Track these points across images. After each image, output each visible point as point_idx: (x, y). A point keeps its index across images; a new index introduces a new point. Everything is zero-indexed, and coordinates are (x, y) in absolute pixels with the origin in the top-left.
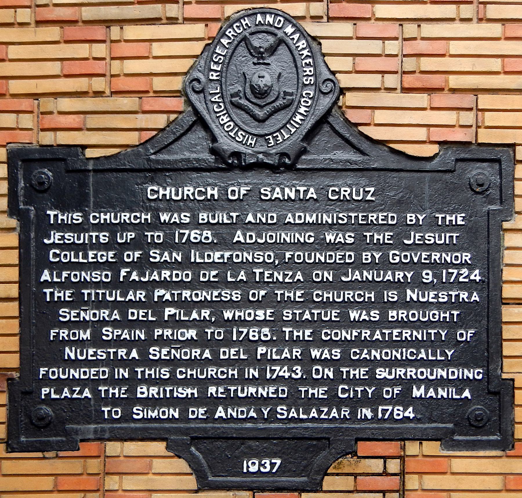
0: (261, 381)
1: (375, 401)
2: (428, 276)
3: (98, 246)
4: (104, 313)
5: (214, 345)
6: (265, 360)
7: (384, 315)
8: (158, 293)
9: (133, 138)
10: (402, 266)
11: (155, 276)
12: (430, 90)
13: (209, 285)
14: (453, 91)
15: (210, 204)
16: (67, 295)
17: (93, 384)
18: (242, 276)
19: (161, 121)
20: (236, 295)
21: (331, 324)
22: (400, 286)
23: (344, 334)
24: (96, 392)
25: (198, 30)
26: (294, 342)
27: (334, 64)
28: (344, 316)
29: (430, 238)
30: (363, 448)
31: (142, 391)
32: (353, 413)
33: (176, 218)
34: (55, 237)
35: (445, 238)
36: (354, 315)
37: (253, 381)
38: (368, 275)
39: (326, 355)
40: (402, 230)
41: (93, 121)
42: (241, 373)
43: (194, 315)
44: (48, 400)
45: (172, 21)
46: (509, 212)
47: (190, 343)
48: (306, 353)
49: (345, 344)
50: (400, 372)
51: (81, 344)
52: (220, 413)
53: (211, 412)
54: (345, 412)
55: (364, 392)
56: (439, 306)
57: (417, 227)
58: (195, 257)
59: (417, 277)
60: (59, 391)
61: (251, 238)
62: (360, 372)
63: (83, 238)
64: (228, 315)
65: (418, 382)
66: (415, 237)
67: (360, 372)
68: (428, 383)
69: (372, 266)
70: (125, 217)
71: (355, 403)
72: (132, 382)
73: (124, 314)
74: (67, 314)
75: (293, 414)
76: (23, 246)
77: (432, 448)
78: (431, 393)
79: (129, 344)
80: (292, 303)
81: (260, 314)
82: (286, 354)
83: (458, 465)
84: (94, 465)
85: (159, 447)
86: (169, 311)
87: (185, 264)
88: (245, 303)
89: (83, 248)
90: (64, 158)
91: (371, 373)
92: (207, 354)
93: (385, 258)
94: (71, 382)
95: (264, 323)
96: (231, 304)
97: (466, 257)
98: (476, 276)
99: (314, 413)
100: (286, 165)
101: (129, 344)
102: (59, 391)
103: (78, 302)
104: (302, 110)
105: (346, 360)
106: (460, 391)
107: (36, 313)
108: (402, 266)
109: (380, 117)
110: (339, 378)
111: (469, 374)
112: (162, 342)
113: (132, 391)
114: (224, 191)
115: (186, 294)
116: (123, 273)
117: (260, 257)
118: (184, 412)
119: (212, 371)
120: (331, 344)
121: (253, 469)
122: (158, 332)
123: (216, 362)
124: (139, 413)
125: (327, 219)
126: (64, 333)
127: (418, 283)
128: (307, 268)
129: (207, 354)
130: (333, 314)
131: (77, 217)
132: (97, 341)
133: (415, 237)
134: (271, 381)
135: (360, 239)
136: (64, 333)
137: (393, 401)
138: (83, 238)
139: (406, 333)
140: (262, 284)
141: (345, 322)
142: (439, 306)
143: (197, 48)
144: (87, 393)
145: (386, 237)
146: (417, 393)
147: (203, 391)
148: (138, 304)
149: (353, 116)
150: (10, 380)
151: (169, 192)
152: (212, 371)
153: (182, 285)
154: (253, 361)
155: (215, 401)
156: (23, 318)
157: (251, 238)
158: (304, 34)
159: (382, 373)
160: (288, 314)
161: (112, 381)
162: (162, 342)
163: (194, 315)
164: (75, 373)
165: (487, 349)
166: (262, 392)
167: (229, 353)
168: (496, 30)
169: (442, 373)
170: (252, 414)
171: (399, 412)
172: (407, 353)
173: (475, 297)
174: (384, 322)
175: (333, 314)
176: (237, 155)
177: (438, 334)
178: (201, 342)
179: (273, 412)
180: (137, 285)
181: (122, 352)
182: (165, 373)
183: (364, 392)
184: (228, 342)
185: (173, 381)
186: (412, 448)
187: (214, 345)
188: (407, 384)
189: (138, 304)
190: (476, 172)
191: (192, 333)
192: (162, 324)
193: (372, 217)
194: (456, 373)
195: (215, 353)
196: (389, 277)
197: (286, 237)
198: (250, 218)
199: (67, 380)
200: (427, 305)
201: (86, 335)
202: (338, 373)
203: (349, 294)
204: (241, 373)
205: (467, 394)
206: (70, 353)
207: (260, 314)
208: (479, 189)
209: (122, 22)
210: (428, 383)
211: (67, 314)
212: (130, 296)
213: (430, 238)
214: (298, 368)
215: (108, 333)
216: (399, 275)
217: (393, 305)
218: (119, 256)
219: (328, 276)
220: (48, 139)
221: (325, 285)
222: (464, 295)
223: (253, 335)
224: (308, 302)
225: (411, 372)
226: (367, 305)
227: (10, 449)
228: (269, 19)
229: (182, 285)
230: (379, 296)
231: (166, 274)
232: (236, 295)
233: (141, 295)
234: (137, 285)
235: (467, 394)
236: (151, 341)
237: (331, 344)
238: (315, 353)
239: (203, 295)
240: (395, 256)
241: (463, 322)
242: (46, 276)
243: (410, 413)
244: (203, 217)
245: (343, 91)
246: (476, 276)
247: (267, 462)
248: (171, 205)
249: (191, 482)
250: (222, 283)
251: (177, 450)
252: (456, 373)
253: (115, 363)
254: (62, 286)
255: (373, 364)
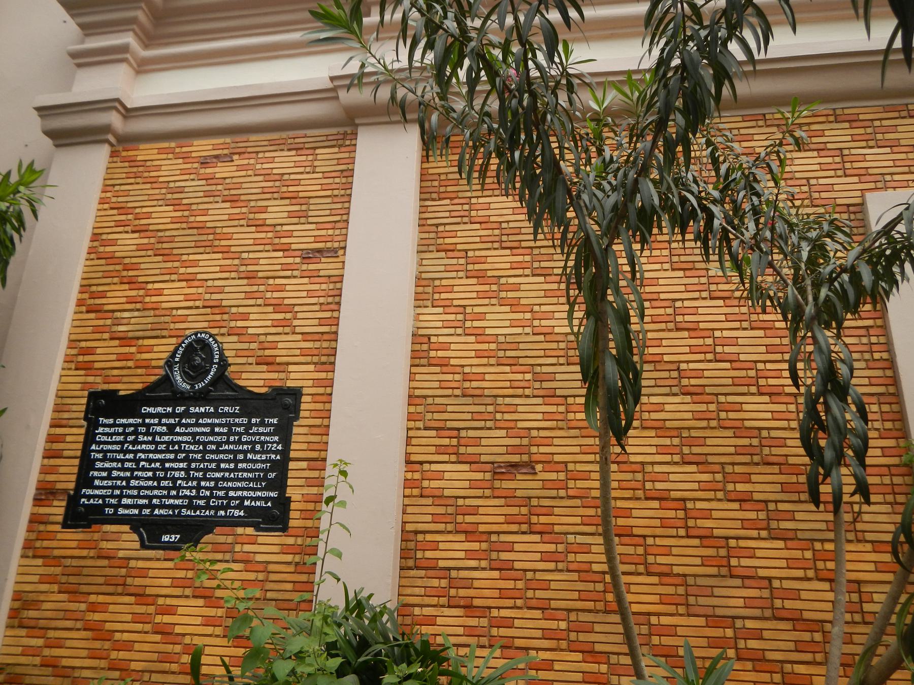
0: (177, 497)
1: (225, 508)
2: (258, 447)
3: (118, 434)
4: (114, 465)
5: (159, 480)
6: (181, 487)
7: (236, 466)
8: (139, 455)
9: (140, 386)
10: (247, 443)
11: (139, 448)
12: (267, 364)
13: (161, 452)
14: (278, 364)
15: (168, 416)
16: (100, 456)
17: (103, 497)
18: (176, 447)
19: (153, 379)
20: (172, 456)
21: (212, 470)
22: (245, 452)
23: (217, 475)
24: (104, 501)
25: (174, 341)
26: (194, 479)
27: (227, 353)
28: (218, 466)
29: (261, 430)
30: (217, 530)
31: (125, 501)
32: (216, 513)
33: (152, 421)
34: (101, 430)
35: (268, 430)
36: (222, 465)
37: (174, 497)
38: (231, 447)
39: (208, 485)
40: (249, 426)
41: (125, 379)
42: (169, 493)
43: (153, 465)
44: (84, 505)
45: (164, 337)
46: (297, 418)
47: (148, 479)
48: (199, 484)
49: (217, 480)
50: (239, 493)
51: (102, 479)
52: (156, 512)
53: (153, 511)
54: (212, 512)
55: (222, 503)
56: (263, 462)
57: (256, 425)
58: (157, 439)
59: (253, 448)
60: (88, 501)
61: (183, 430)
62: (221, 493)
63: (112, 430)
64: (167, 465)
65: (248, 498)
66: (254, 429)
67: (221, 493)
68: (252, 499)
69: (234, 443)
70: (131, 421)
71: (217, 508)
72: (120, 497)
73: (123, 465)
74: (99, 465)
75: (189, 513)
76: (87, 434)
77: (250, 530)
78: (253, 503)
79: (122, 479)
80: (195, 460)
81: (182, 465)
82: (190, 484)
83: (260, 540)
84: (96, 536)
85: (126, 528)
86: (142, 463)
87: (153, 442)
88: (176, 460)
89: (111, 435)
90: (111, 395)
91: (227, 494)
92: (155, 484)
93: (240, 439)
94: (94, 496)
95: (182, 469)
96: (170, 461)
97: (276, 438)
98: (280, 447)
99: (198, 513)
100: (201, 397)
101: (122, 479)
102: (88, 501)
103: (104, 460)
104: (212, 373)
105: (216, 488)
106: (266, 503)
107: (86, 463)
108: (247, 443)
109: (244, 376)
110: (212, 496)
111: (272, 494)
112: (137, 478)
113: (120, 501)
114: (174, 410)
115: (151, 455)
116: (126, 445)
117: (185, 438)
118: (140, 512)
119: (156, 492)
120: (210, 479)
121: (167, 540)
122: (136, 473)
123: (159, 488)
124: (121, 511)
125: (217, 421)
126: (96, 474)
127: (253, 451)
128: (205, 444)
129: (155, 484)
130: (213, 465)
131: (111, 421)
132: (109, 478)
133: (254, 429)
134: (181, 497)
135: (230, 430)
136: (96, 474)
137: (235, 508)
138: (112, 430)
139: (245, 475)
140: (184, 451)
141: (218, 469)
142: (263, 462)
143: (172, 348)
144: (100, 502)
145: (241, 429)
146: (247, 503)
147: (150, 501)
148: (129, 460)
149: (232, 376)
150: (69, 495)
151: (151, 410)
152: (156, 492)
153: (150, 451)
154: (174, 487)
155: (155, 506)
156: (81, 467)
157: (183, 430)
158: (216, 342)
159: (231, 494)
160: (193, 465)
161: (112, 496)
162: (137, 478)
163: (153, 465)
164: (97, 492)
165: (280, 484)
166: (177, 502)
167: (164, 483)
168: (299, 337)
169: (259, 494)
170: (171, 513)
171: (237, 513)
172: (244, 484)
173: (278, 457)
174: (236, 470)
175: (213, 465)
176: (182, 393)
177: (259, 475)
178: (153, 478)
179: (180, 512)
180: (131, 452)
181: (119, 482)
182: (135, 492)
183: (222, 503)
184: (165, 478)
185: (139, 497)
186: (240, 530)
187: (159, 480)
188: (242, 499)
189: (129, 460)
190: (289, 400)
191: (150, 474)
192: (138, 469)
193: (237, 420)
194: (265, 494)
195: (159, 483)
196: (241, 448)
197: (199, 430)
198: (184, 421)
199: (92, 496)
200: (256, 461)
201: (105, 474)
202: (212, 493)
203: (221, 456)
204: (169, 493)
205: (269, 504)
206: (97, 482)
207: (182, 465)
208: (286, 408)
209: (144, 338)
210: (252, 499)
211: (99, 465)
212: (127, 456)
213: (261, 430)
214: (194, 491)
215: (115, 473)
216: (245, 447)
217: (242, 461)
218: (125, 438)
219: (214, 447)
220: (106, 387)
221: (212, 452)
222: (273, 456)
223: (177, 474)
224: (203, 460)
225: (245, 493)
226: (228, 461)
227: (63, 527)
228: (203, 335)
229: (150, 451)
230: (235, 457)
231: (144, 446)
232: (172, 456)
233: (131, 456)
234: (131, 452)
235: (269, 504)
236: (132, 477)
237: (210, 479)
238: (203, 484)
239: (158, 456)
240: (244, 438)
241: (271, 470)
242: (93, 447)
243: (242, 513)
244: (164, 421)
245: (230, 365)
246: (280, 447)
247: (173, 536)
248: (151, 416)
249: (137, 545)
250: (167, 451)
251: (135, 529)
252: (265, 494)
253: (113, 488)
254: (98, 452)
255: (228, 489)
